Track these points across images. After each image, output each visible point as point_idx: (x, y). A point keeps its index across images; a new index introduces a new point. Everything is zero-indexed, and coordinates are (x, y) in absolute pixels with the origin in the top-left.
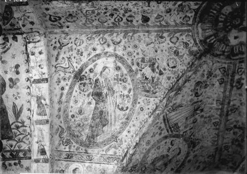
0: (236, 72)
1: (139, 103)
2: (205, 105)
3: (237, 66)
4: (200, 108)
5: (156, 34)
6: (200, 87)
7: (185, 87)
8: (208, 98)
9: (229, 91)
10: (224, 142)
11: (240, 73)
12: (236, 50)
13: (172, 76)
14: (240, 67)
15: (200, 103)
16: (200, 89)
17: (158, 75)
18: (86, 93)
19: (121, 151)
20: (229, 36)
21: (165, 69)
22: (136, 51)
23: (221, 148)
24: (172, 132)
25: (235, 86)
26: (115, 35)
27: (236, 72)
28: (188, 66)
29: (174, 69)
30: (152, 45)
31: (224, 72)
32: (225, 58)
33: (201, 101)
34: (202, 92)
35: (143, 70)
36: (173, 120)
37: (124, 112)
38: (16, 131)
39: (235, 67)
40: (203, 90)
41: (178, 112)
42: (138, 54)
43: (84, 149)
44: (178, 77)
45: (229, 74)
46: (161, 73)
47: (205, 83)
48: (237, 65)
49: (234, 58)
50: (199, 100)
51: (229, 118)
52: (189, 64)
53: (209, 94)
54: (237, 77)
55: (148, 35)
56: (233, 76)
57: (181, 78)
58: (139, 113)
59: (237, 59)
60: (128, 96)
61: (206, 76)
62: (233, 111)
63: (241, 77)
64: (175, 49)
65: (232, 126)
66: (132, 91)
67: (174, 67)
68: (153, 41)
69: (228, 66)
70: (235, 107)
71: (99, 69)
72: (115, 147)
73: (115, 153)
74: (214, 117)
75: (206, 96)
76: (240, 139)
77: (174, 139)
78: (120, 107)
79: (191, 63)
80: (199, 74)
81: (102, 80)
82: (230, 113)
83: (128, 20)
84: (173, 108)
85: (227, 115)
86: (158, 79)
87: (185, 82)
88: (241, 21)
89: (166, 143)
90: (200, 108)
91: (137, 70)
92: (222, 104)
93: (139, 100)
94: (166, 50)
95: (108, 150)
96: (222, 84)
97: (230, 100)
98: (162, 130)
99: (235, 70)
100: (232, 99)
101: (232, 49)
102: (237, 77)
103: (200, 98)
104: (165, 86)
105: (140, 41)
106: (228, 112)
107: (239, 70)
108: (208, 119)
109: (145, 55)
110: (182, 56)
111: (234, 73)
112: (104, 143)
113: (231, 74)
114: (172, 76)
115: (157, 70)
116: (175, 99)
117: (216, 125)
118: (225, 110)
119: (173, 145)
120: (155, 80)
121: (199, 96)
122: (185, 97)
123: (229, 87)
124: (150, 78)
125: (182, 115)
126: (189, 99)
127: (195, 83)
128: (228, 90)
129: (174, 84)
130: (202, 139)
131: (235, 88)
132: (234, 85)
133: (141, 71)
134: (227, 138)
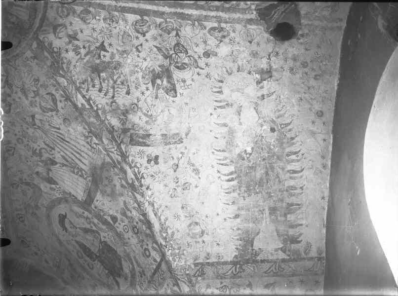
62: (11, 153)
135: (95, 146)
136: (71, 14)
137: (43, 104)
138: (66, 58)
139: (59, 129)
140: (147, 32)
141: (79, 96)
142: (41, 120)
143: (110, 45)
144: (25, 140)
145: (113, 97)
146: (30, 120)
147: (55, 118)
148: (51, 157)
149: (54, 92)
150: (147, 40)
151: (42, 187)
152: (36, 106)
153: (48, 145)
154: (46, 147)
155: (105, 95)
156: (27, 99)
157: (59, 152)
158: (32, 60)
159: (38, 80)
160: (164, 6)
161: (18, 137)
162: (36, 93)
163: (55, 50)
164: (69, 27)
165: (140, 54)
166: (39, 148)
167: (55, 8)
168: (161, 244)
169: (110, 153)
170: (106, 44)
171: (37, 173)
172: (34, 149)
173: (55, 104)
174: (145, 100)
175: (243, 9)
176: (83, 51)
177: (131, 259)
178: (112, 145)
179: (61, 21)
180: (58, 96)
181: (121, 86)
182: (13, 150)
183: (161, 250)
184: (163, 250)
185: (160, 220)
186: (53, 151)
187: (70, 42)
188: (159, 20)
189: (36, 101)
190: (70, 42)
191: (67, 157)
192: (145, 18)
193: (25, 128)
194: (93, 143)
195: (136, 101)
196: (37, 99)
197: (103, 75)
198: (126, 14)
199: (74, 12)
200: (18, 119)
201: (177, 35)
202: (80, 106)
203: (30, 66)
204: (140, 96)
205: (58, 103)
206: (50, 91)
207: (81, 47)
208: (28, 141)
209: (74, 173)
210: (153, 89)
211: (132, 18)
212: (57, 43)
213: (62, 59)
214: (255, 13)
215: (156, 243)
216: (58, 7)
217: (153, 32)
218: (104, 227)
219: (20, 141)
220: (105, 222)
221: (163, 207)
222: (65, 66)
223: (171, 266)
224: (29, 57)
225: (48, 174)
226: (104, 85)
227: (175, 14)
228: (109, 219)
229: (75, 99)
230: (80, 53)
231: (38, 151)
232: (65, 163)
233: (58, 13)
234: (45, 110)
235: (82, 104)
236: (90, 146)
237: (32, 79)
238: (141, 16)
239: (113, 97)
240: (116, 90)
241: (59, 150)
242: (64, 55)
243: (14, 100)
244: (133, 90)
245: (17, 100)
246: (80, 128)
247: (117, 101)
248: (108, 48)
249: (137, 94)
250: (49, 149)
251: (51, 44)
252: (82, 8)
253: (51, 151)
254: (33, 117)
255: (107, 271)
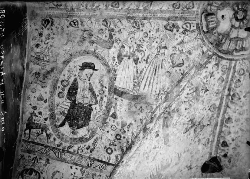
0: (186, 22)
3: (193, 22)
9: (162, 16)
10: (84, 19)
11: (185, 26)
12: (212, 18)
14: (192, 25)
20: (227, 9)
23: (72, 16)
25: (169, 23)
27: (186, 22)
31: (188, 7)
32: (204, 6)
39: (192, 19)
45: (183, 13)
48: (194, 22)
49: (203, 17)
51: (124, 22)
54: (180, 23)
56: (181, 18)
59: (201, 21)
62: (134, 25)
63: (180, 28)
65: (112, 26)
69: (194, 11)
70: (140, 26)
76: (93, 38)
82: (132, 21)
85: (128, 18)
88: (240, 19)
96: (173, 7)
97: (150, 19)
99: (189, 20)
100: (151, 21)
101: (213, 14)
102: (180, 23)
106: (133, 18)
107: (188, 25)
111: (185, 19)
113: (183, 16)
118: (135, 15)
123: (167, 15)
128: (163, 15)
131: (165, 23)
132: (170, 21)
134: (91, 22)
135: (160, 97)
136: (223, 73)
137: (175, 56)
138: (203, 72)
139: (162, 67)
140: (210, 110)
141: (186, 83)
142: (164, 53)
143: (207, 94)
144: (147, 39)
145: (184, 102)
146: (163, 44)
147: (168, 65)
148: (140, 60)
149: (185, 65)
150: (207, 111)
151: (112, 50)
152: (173, 51)
153: (148, 58)
154: (146, 56)
155: (186, 97)
156: (177, 45)
157: (145, 67)
158: (201, 51)
159: (190, 54)
160: (222, 117)
161: (149, 33)
162: (182, 51)
163: (207, 65)
164: (217, 72)
165: (202, 110)
166: (144, 49)
167: (226, 64)
168: (123, 161)
169: (158, 109)
170: (208, 92)
171: (123, 47)
172: (142, 46)
173: (177, 66)
174: (183, 119)
175: (217, 151)
176: (205, 81)
177: (93, 136)
178: (164, 109)
179: (220, 67)
180: (183, 68)
181: (189, 104)
182: (137, 27)
183: (119, 162)
184: (120, 164)
185: (134, 154)
186: (145, 62)
187: (210, 73)
188: (215, 116)
189: (176, 51)
190: (210, 73)
191: (143, 73)
192: (217, 109)
193: (156, 40)
194: (161, 95)
195: (182, 114)
196: (178, 52)
197: (194, 94)
198: (220, 100)
199: (223, 74)
200: (162, 36)
201: (208, 125)
202: (181, 84)
203: (198, 49)
204: (184, 116)
205: (179, 68)
206: (185, 62)
207: (207, 80)
208: (147, 42)
209: (134, 79)
210: (188, 121)
211: (218, 103)
212: (210, 66)
213: (202, 70)
214: (215, 156)
215: (122, 158)
216: (227, 66)
217: (210, 113)
218: (104, 107)
219: (146, 35)
220: (108, 110)
221: (139, 152)
222: (199, 72)
223: (114, 174)
224: (203, 49)
225: (125, 56)
226: (190, 96)
227: (217, 123)
228: (112, 111)
229: (184, 81)
230: (204, 78)
231: (141, 49)
232: (139, 72)
233: (224, 66)
234: (172, 57)
235: (182, 86)
236: (159, 94)
237: (190, 50)
238: (218, 107)
239: (184, 102)
240: (187, 102)
241: (147, 67)
242: (205, 70)
243: (175, 34)
244: (187, 111)
245: (176, 37)
246: (167, 85)
247: (183, 104)
248: (206, 93)
249: (186, 114)
250: (145, 58)
251: (210, 62)
252: (224, 78)
253: (144, 60)
254: (165, 48)
255: (66, 112)
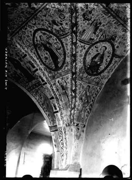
1: (64, 42)
2: (99, 20)
4: (98, 23)
5: (44, 9)
6: (87, 15)
7: (78, 22)
8: (97, 16)
13: (67, 22)
15: (95, 22)
16: (88, 16)
17: (60, 26)
18: (43, 50)
19: (70, 67)
21: (61, 21)
22: (44, 22)
24: (91, 43)
26: (31, 21)
28: (70, 12)
29: (65, 19)
30: (47, 15)
33: (95, 20)
34: (91, 16)
35: (54, 28)
36: (87, 38)
37: (61, 50)
38: (33, 76)
40: (90, 15)
41: (85, 34)
42: (46, 23)
43: (56, 72)
44: (70, 20)
46: (61, 24)
47: (88, 12)
50: (93, 21)
52: (69, 11)
53: (96, 14)
55: (42, 12)
57: (72, 19)
58: (67, 47)
60: (57, 42)
61: (85, 9)
64: (57, 10)
66: (57, 39)
67: (64, 17)
68: (46, 13)
71: (39, 39)
72: (67, 66)
73: (68, 68)
74: (112, 21)
75: (96, 16)
77: (96, 45)
78: (58, 48)
79: (70, 10)
80: (80, 11)
81: (43, 42)
82: (118, 14)
83: (28, 14)
84: (81, 34)
86: (63, 27)
87: (76, 20)
89: (92, 49)
90: (98, 23)
91: (51, 29)
92: (109, 12)
93: (63, 41)
94: (54, 13)
95: (65, 68)
98: (84, 46)
103: (92, 20)
104: (68, 28)
105: (41, 17)
108: (109, 24)
109: (48, 21)
110: (63, 10)
112: (62, 67)
114: (67, 22)
115: (59, 24)
116: (78, 30)
117: (117, 23)
119: (98, 48)
120: (62, 29)
121: (91, 19)
122: (83, 25)
124: (59, 29)
125: (90, 33)
126: (86, 25)
127: (82, 16)
129: (71, 25)
130: (116, 34)
133: (53, 29)
